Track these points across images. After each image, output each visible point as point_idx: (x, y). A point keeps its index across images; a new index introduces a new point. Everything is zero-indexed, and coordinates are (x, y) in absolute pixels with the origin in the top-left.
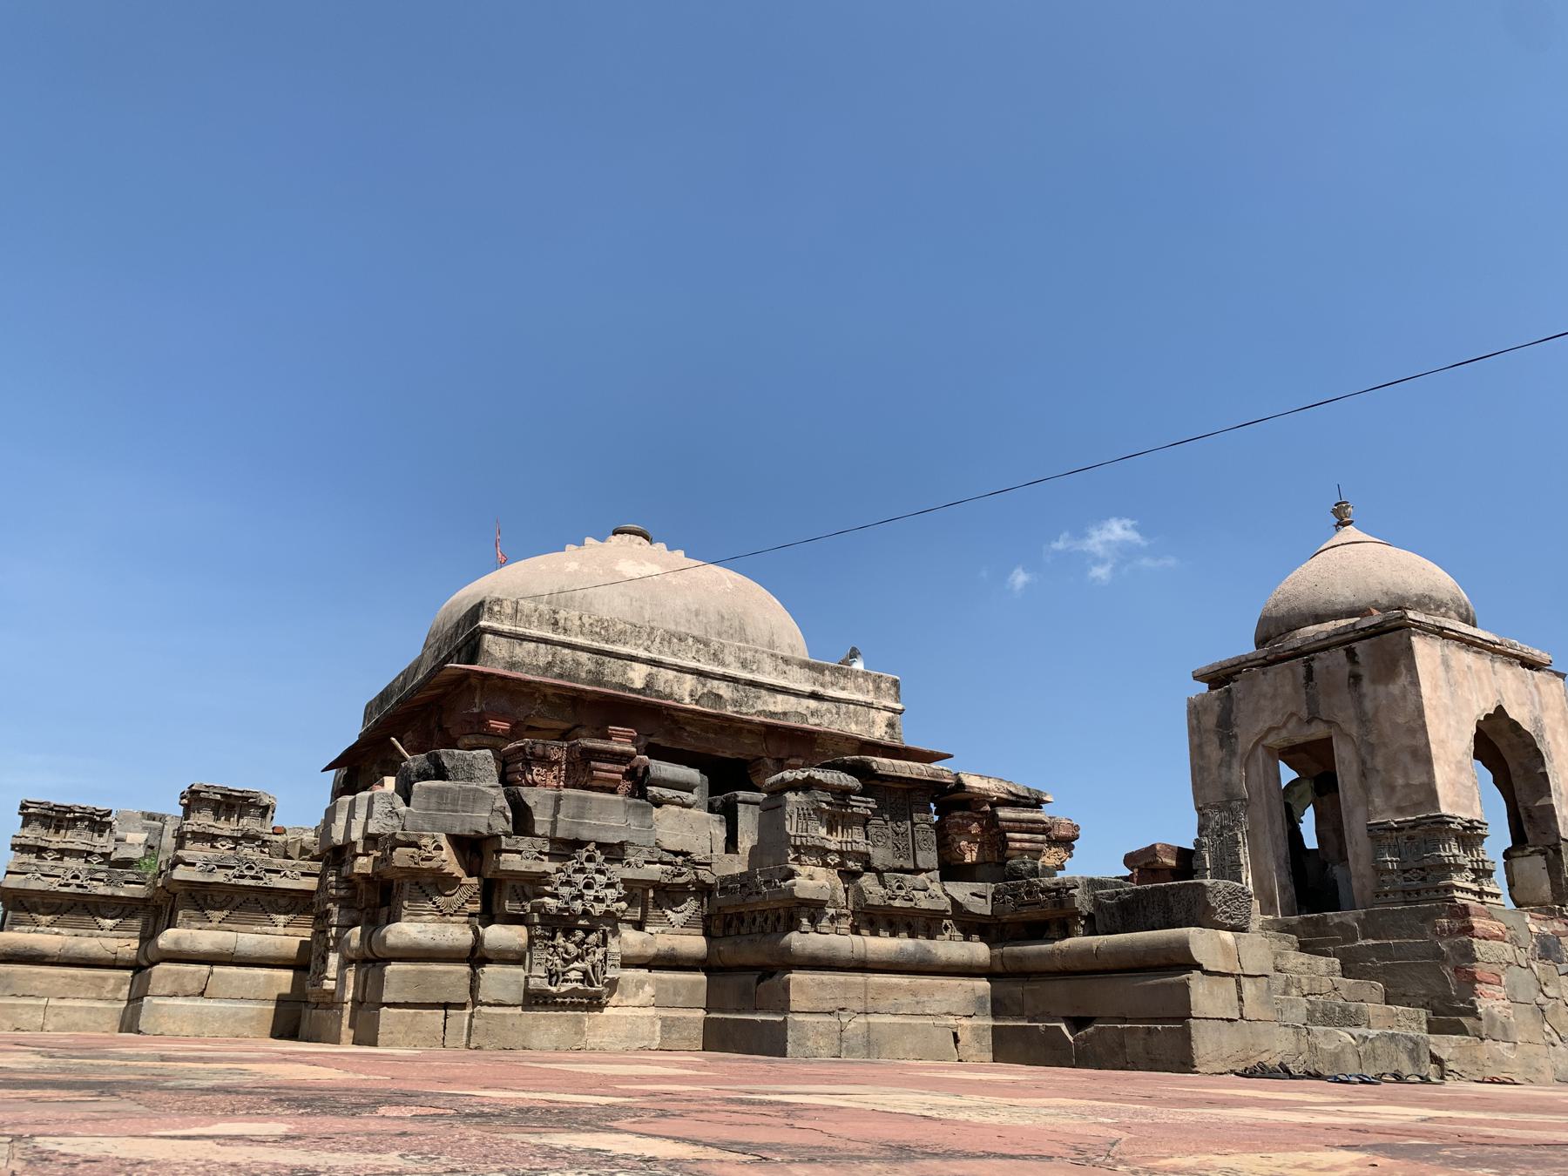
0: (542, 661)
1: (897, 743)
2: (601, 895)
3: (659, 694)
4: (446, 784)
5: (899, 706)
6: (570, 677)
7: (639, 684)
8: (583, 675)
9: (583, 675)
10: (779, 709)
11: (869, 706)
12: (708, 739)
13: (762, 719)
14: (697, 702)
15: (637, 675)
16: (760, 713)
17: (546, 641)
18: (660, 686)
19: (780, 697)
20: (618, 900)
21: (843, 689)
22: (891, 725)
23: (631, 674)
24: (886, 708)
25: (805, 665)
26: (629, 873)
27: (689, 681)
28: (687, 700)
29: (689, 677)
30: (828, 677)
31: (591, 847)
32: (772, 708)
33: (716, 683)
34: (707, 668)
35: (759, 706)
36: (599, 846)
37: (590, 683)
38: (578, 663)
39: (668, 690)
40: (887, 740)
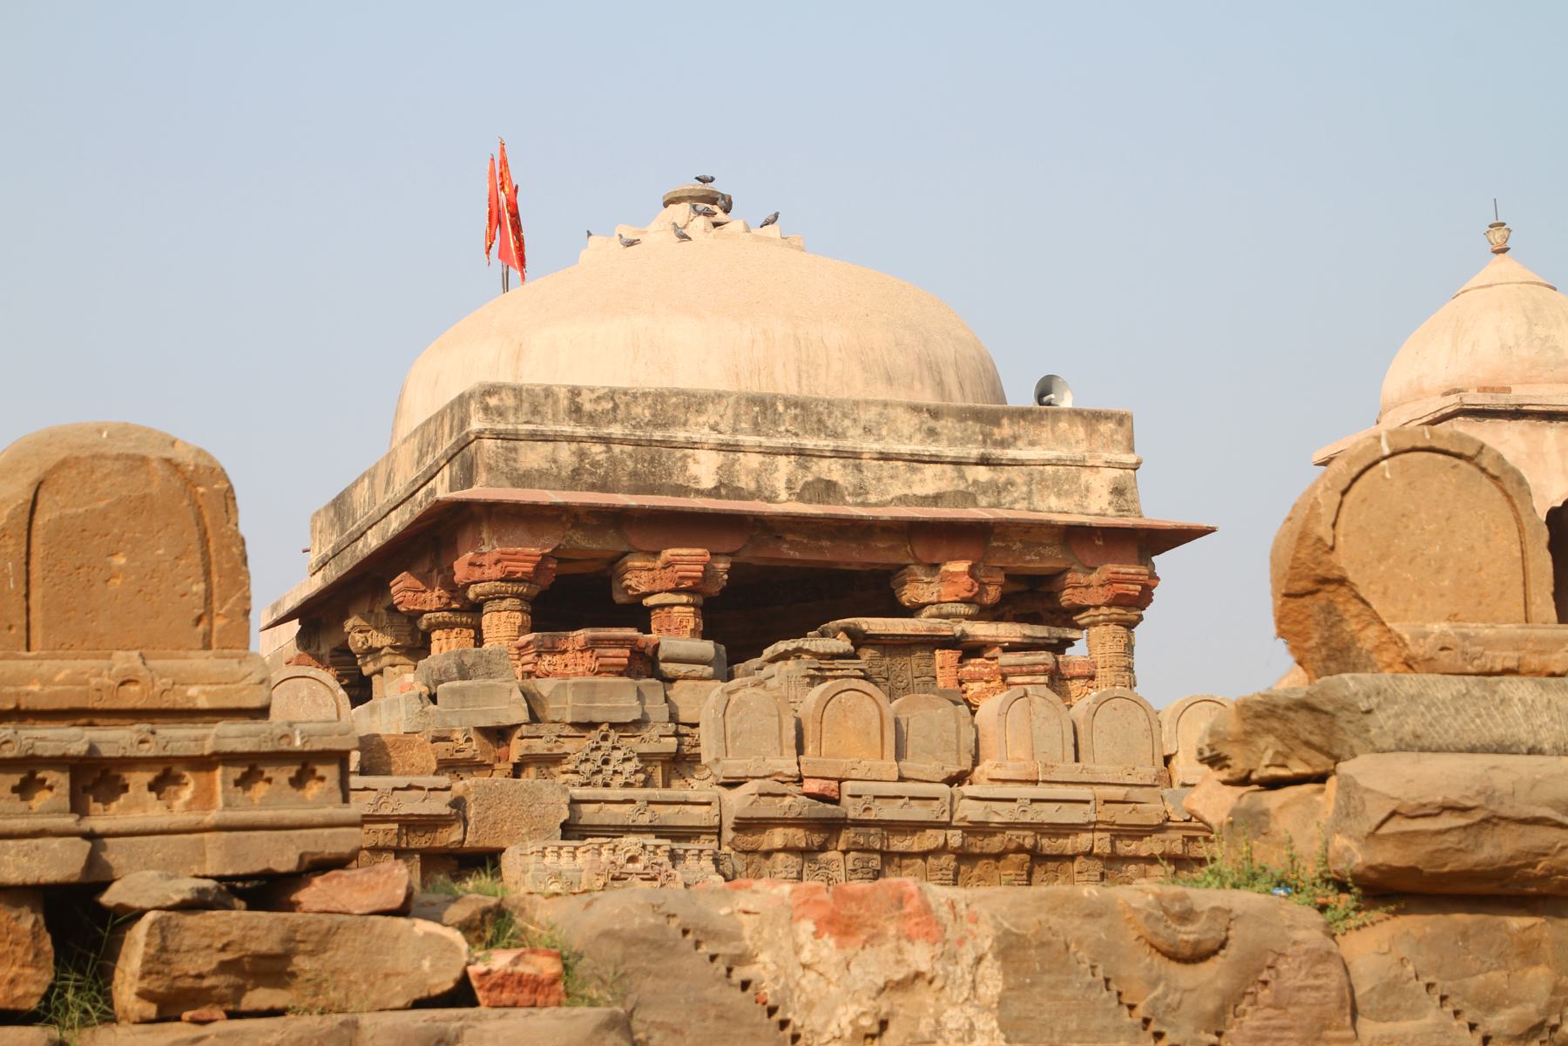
1: (1130, 521)
2: (619, 768)
3: (738, 494)
4: (466, 683)
5: (1130, 459)
6: (603, 487)
7: (708, 483)
8: (625, 481)
9: (625, 481)
10: (930, 489)
11: (1081, 464)
14: (800, 498)
15: (704, 469)
16: (903, 500)
17: (571, 439)
18: (746, 482)
19: (930, 470)
20: (636, 772)
21: (1032, 444)
22: (1118, 491)
23: (693, 469)
24: (1109, 465)
25: (963, 415)
26: (645, 748)
27: (784, 465)
28: (784, 495)
29: (782, 461)
30: (1006, 430)
31: (604, 727)
32: (919, 490)
33: (825, 463)
34: (809, 443)
35: (897, 490)
36: (613, 726)
37: (636, 490)
38: (613, 461)
39: (753, 486)
40: (1113, 519)
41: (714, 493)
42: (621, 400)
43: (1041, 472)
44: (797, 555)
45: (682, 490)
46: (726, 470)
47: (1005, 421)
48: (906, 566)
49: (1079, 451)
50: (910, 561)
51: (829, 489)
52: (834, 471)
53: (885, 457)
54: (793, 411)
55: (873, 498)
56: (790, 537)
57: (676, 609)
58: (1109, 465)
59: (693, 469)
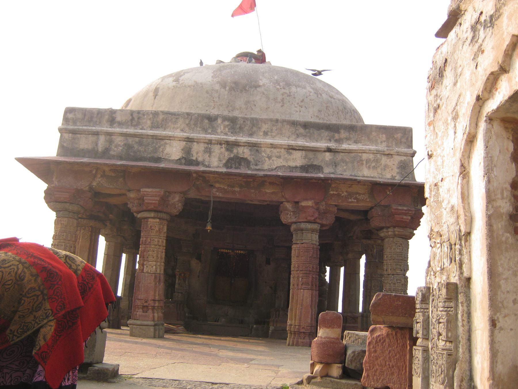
0: (100, 148)
12: (234, 192)
13: (280, 174)
24: (399, 154)
30: (343, 134)
32: (292, 164)
41: (179, 161)
42: (135, 115)
43: (361, 157)
44: (221, 195)
45: (158, 160)
46: (188, 151)
47: (342, 131)
48: (282, 203)
49: (382, 147)
50: (284, 200)
51: (240, 161)
52: (245, 152)
53: (273, 146)
54: (227, 123)
55: (266, 167)
56: (217, 185)
57: (150, 220)
58: (399, 154)
59: (168, 150)
